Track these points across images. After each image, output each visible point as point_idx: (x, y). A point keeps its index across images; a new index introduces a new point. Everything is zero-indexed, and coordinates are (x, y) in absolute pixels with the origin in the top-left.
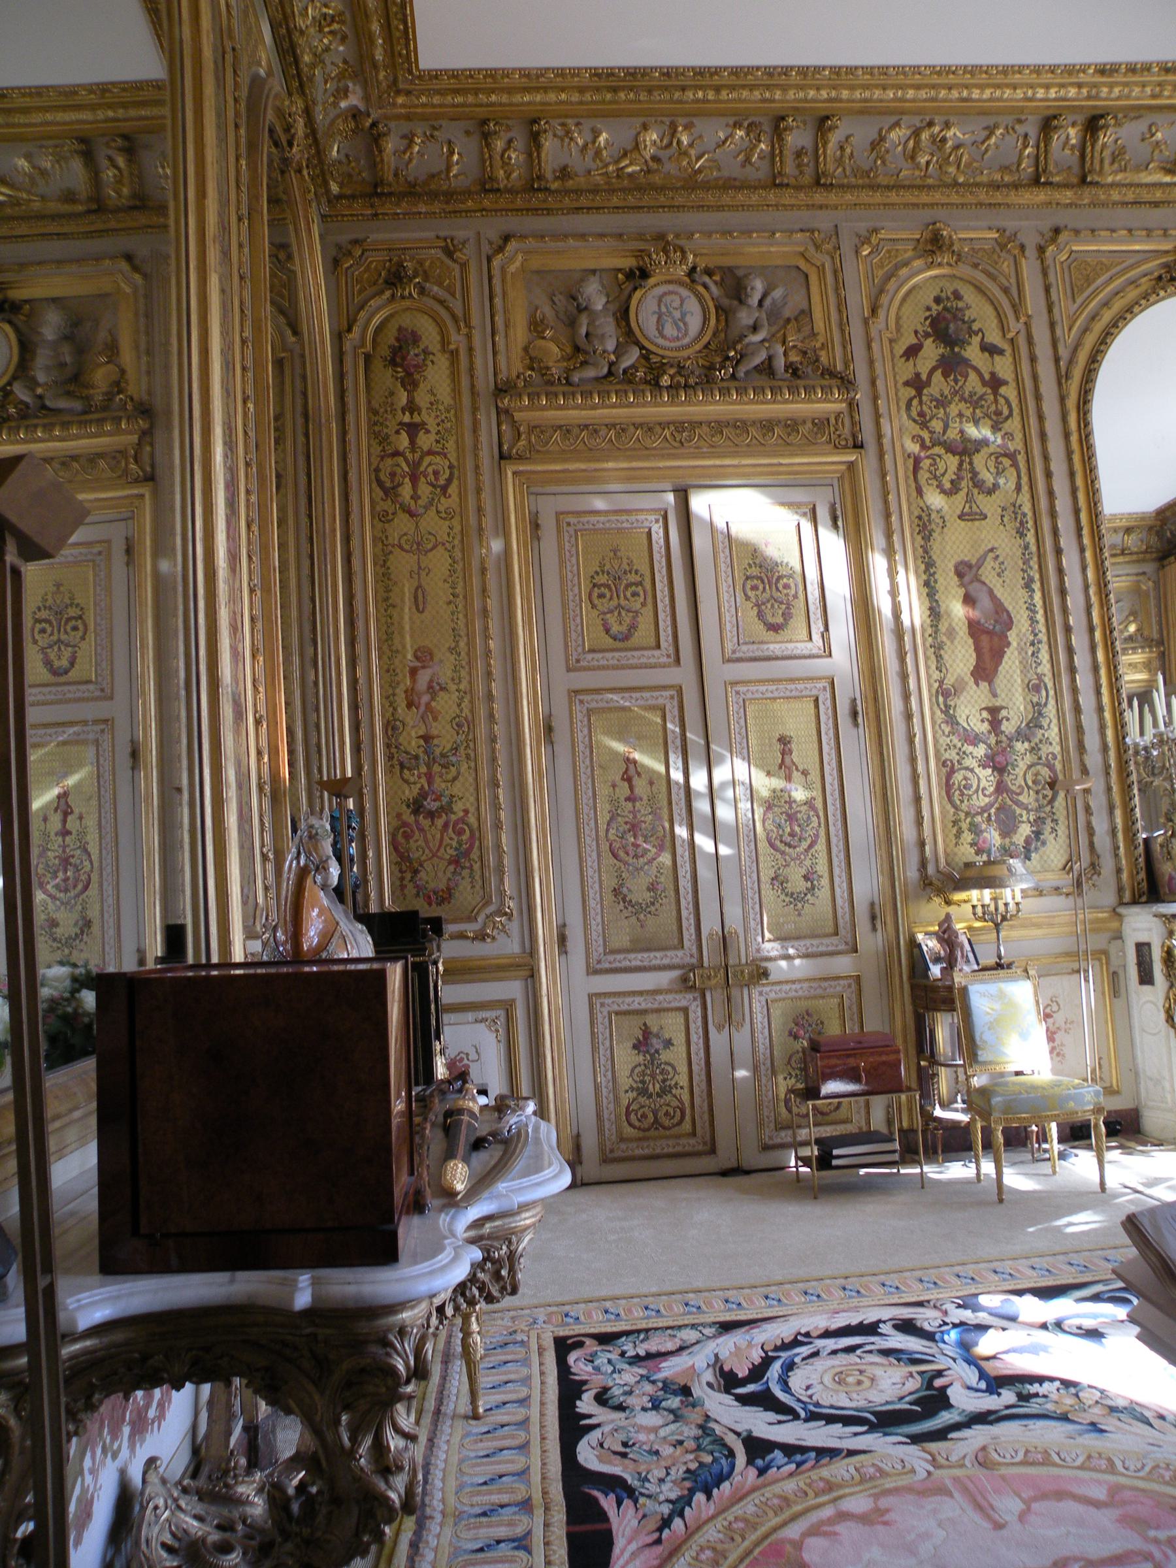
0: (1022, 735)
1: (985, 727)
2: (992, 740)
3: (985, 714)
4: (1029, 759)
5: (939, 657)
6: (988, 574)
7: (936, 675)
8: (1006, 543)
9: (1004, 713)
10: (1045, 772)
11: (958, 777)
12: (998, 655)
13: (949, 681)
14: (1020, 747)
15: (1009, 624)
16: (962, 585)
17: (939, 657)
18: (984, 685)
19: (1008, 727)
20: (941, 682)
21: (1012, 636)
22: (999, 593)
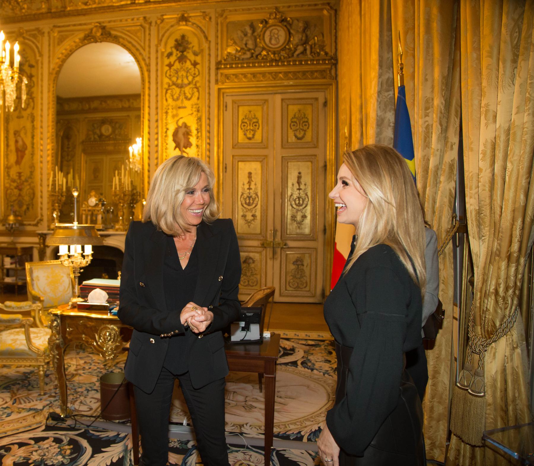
0: (26, 181)
1: (17, 178)
2: (19, 181)
3: (18, 174)
4: (28, 187)
5: (7, 158)
6: (22, 135)
7: (6, 163)
8: (29, 125)
9: (22, 174)
10: (31, 191)
11: (9, 191)
12: (22, 157)
13: (9, 164)
14: (25, 184)
15: (26, 149)
16: (15, 137)
17: (7, 158)
18: (18, 166)
19: (23, 178)
20: (7, 165)
21: (27, 152)
22: (25, 140)
